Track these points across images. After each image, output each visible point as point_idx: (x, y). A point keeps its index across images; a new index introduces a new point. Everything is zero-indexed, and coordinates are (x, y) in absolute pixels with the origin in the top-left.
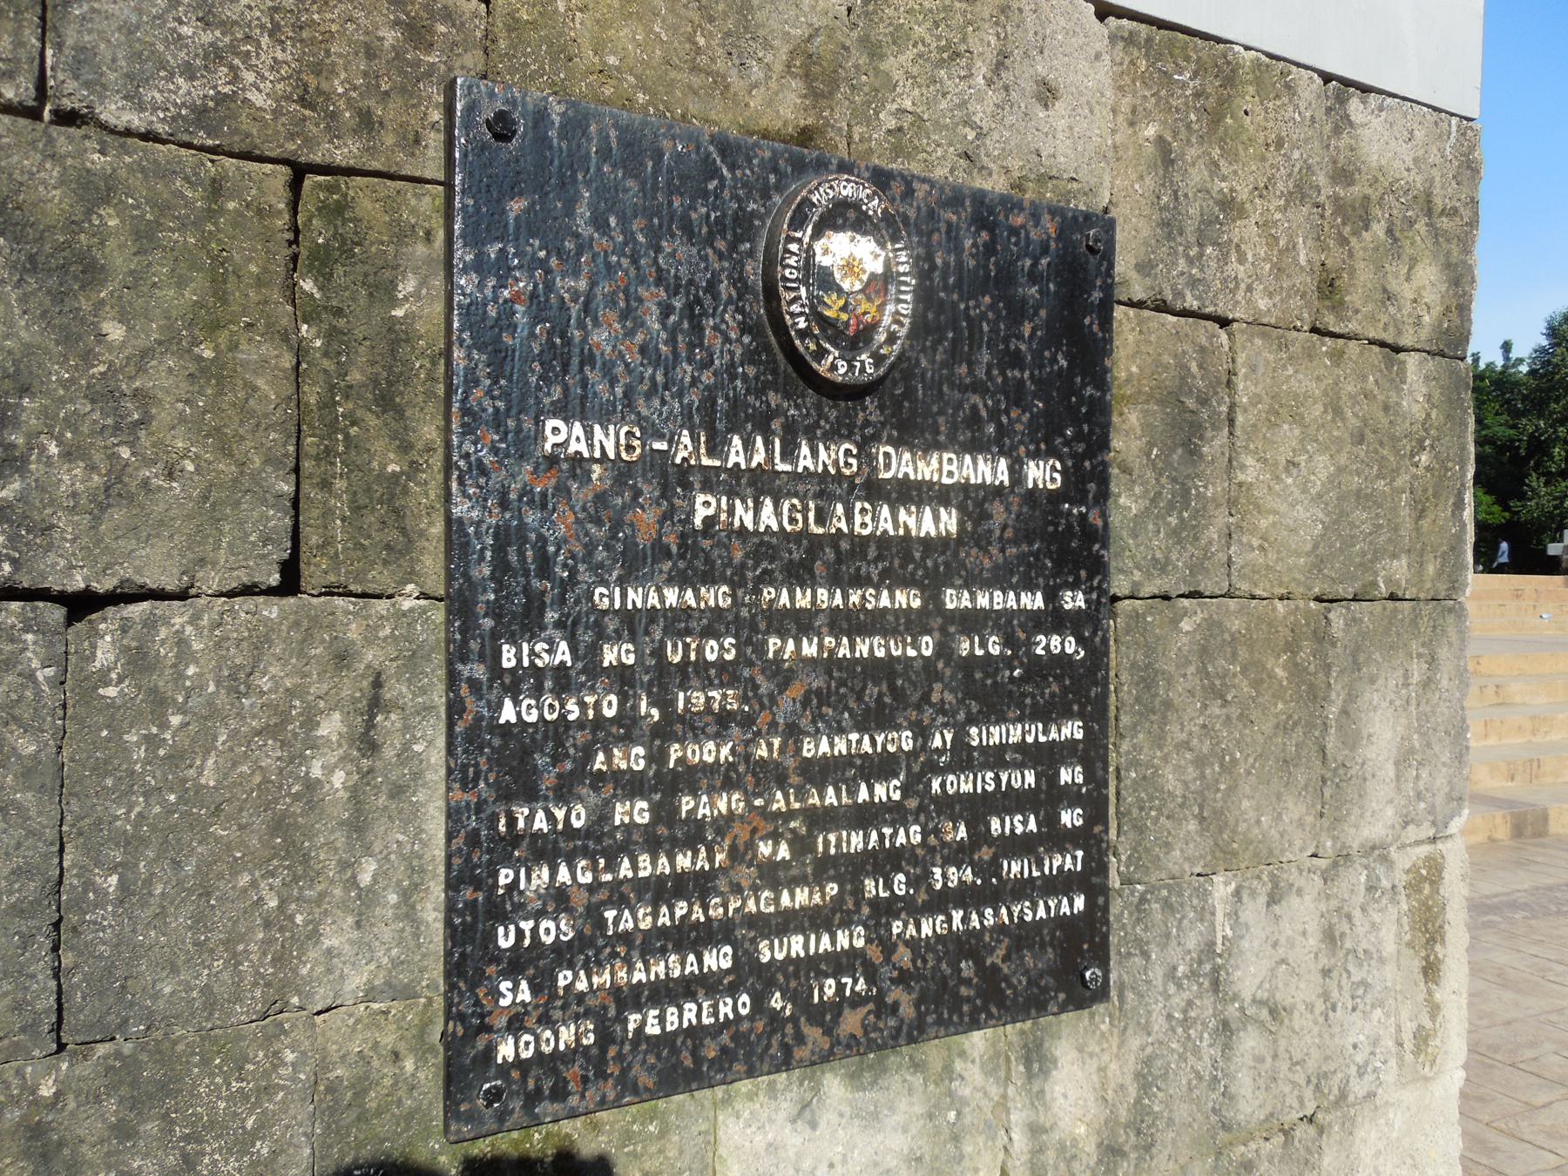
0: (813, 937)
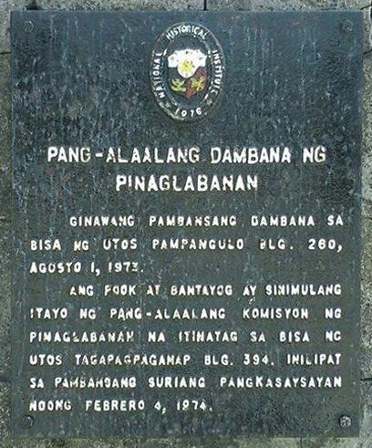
0: (176, 379)
